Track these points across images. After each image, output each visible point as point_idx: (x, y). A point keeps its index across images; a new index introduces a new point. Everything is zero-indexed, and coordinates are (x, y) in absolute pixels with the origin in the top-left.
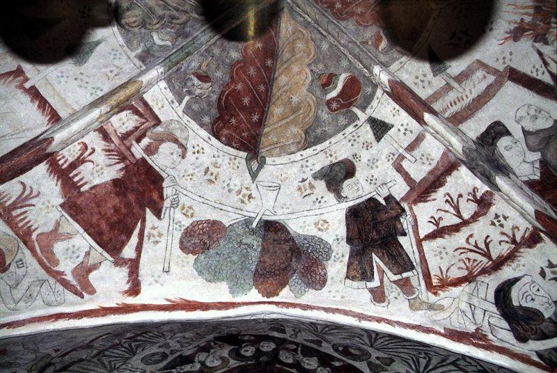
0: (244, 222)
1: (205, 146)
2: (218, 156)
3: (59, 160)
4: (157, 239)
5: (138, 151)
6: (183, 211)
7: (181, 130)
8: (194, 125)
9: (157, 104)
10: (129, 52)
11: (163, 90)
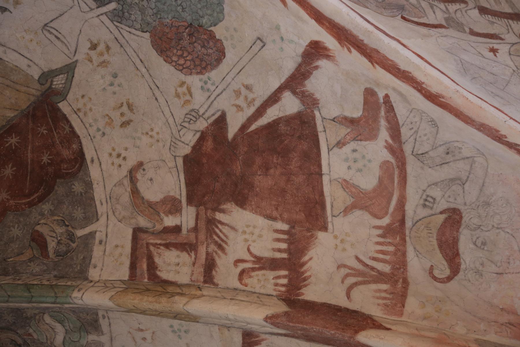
0: (124, 21)
1: (105, 158)
2: (98, 130)
3: (283, 285)
4: (244, 91)
6: (188, 97)
7: (118, 200)
8: (99, 193)
9: (121, 255)
11: (100, 265)
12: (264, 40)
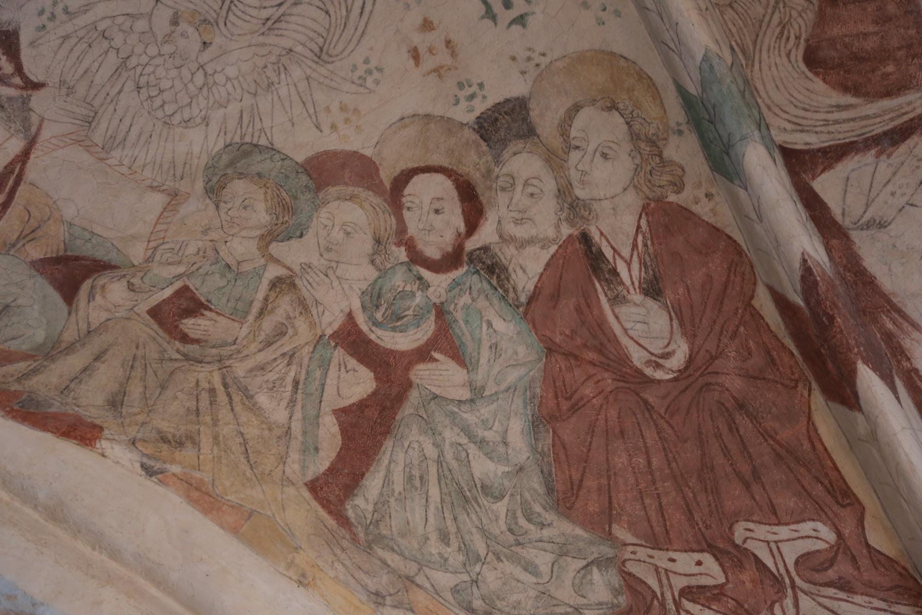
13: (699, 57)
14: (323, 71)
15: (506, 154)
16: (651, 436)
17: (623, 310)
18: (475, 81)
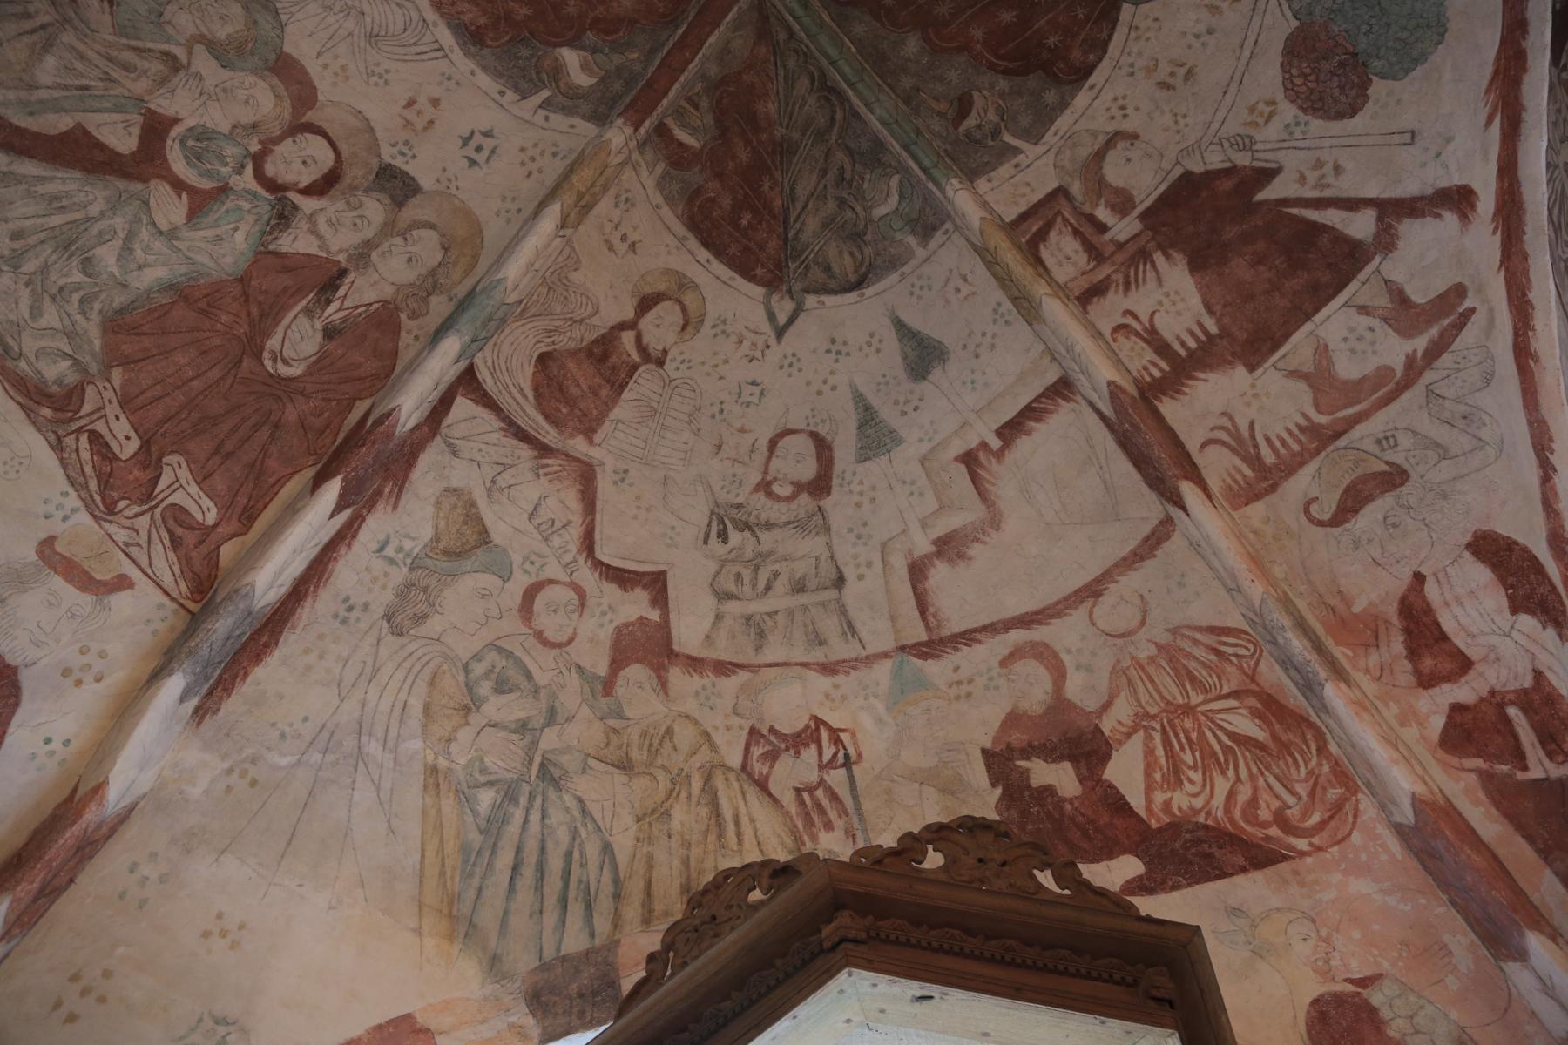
1: (1107, 96)
2: (1132, 65)
3: (1151, 375)
4: (1328, 168)
5: (1124, 228)
6: (1261, 121)
8: (1063, 122)
9: (1024, 195)
10: (914, 262)
11: (995, 183)
12: (1416, 140)
13: (499, 276)
14: (362, 44)
15: (375, 194)
16: (215, 373)
17: (303, 319)
18: (415, 151)
